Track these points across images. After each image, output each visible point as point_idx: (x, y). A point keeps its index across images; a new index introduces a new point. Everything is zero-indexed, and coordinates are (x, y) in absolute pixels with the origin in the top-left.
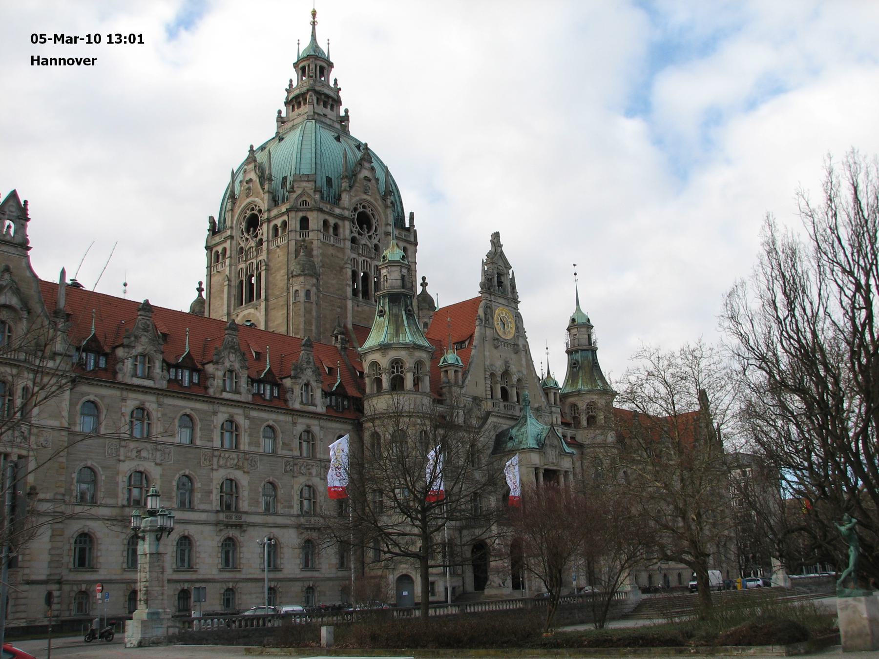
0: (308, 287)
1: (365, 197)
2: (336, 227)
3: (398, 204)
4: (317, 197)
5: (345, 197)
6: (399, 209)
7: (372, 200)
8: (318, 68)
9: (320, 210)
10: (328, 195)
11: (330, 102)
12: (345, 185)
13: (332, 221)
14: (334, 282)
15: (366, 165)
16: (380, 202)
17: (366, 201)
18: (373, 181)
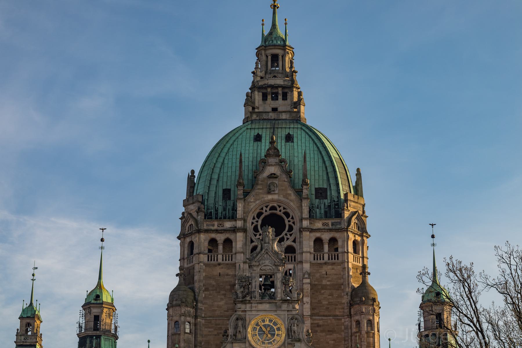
0: (176, 318)
1: (270, 197)
2: (228, 242)
3: (333, 187)
4: (200, 217)
5: (240, 207)
6: (334, 193)
7: (281, 198)
8: (270, 57)
9: (199, 231)
10: (225, 209)
11: (280, 90)
12: (240, 192)
13: (220, 238)
14: (222, 303)
15: (272, 160)
16: (293, 197)
17: (273, 201)
18: (284, 177)
